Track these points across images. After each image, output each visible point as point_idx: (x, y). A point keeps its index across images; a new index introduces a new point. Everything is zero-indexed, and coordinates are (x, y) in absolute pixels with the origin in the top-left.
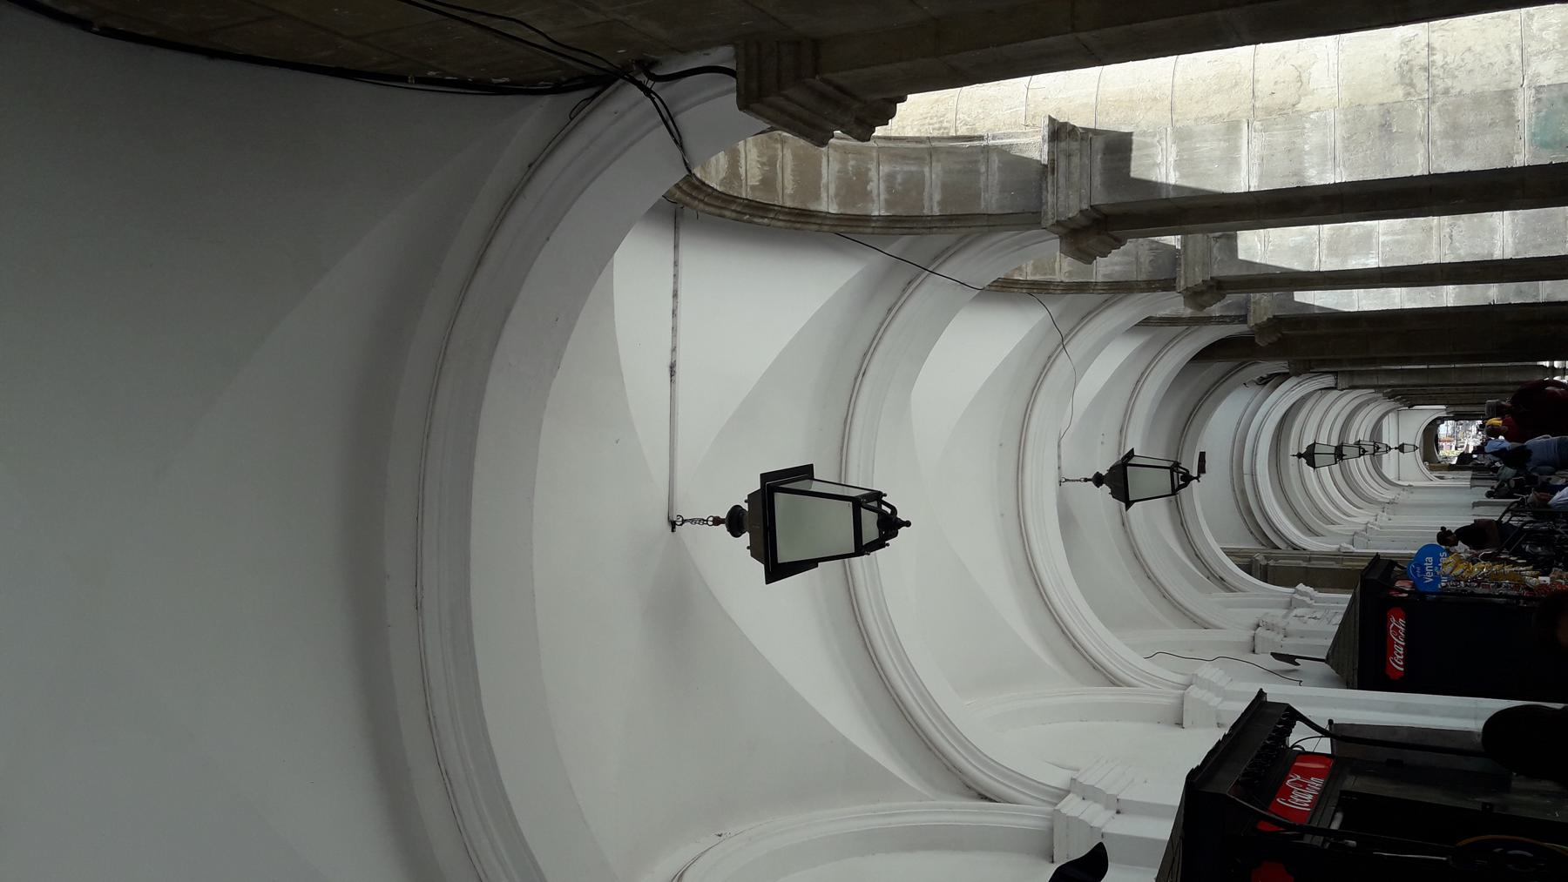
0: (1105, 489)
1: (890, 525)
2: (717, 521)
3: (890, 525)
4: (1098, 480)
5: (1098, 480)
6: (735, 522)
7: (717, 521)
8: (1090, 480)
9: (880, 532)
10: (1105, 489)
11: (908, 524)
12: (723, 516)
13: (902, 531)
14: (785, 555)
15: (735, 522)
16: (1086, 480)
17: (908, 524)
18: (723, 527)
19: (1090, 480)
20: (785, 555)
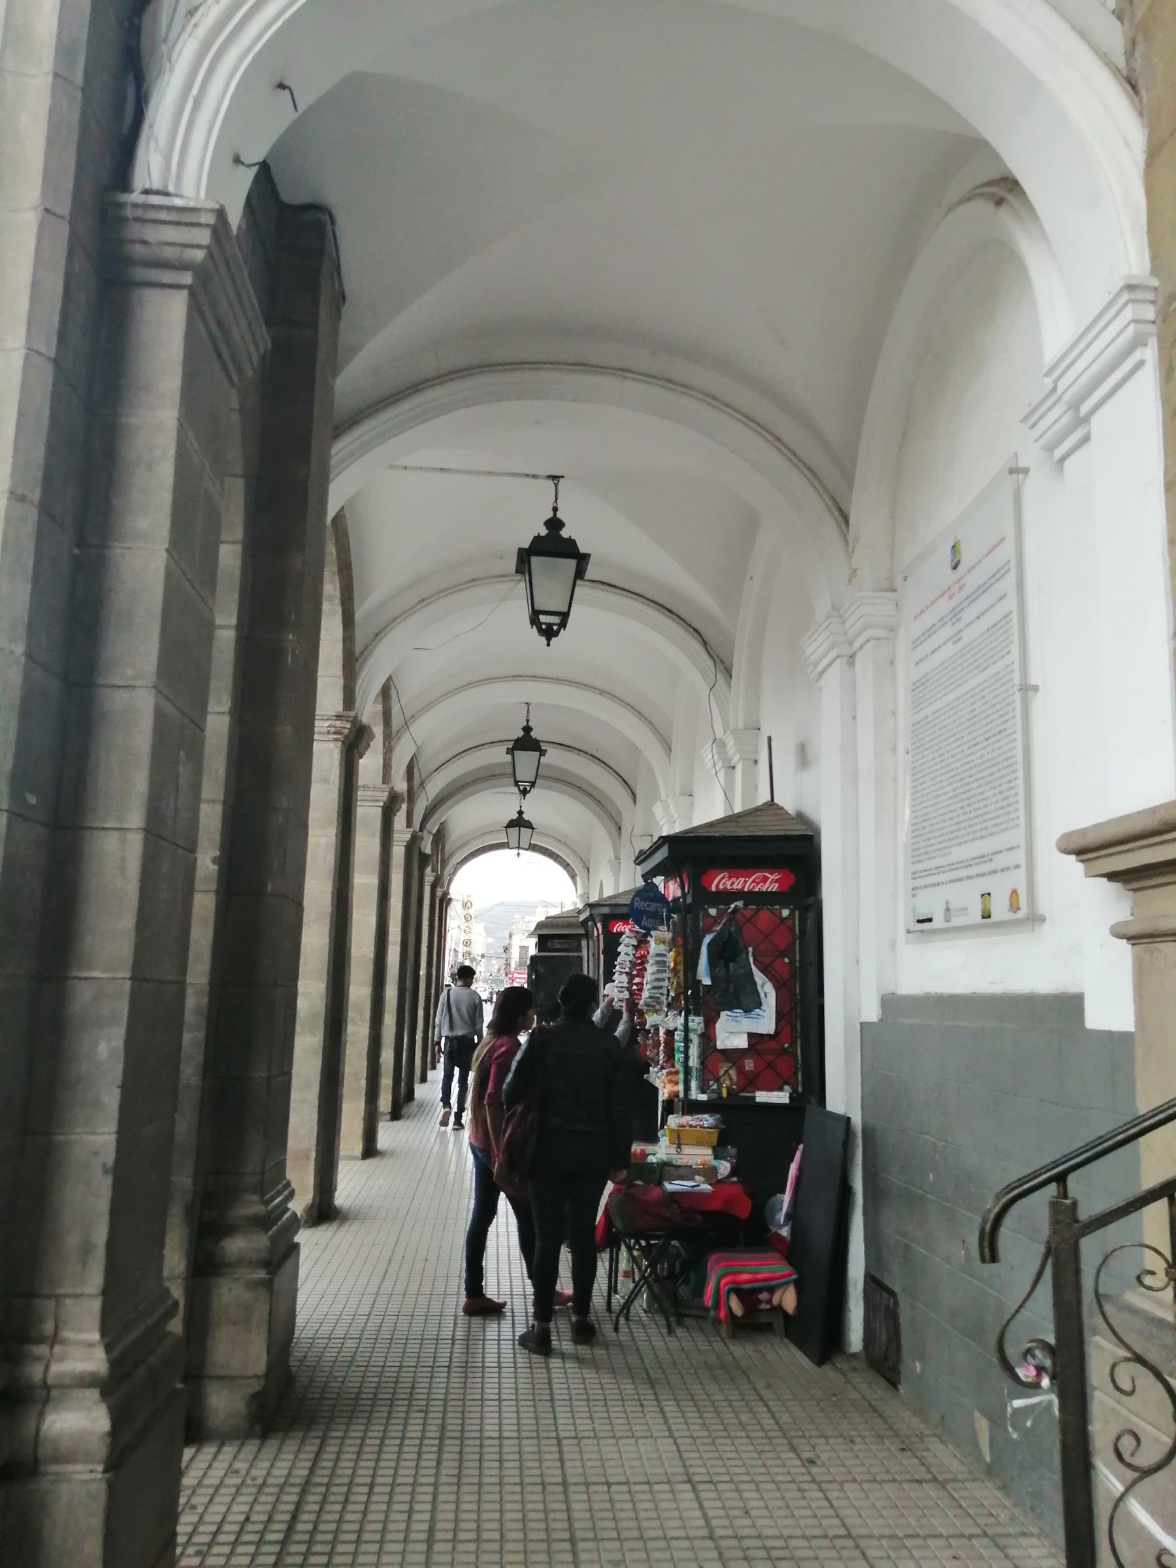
0: (521, 734)
1: (549, 633)
2: (555, 509)
3: (549, 633)
4: (527, 729)
5: (527, 729)
6: (554, 524)
7: (555, 509)
9: (544, 624)
10: (521, 734)
11: (548, 645)
12: (559, 515)
13: (543, 640)
14: (535, 560)
15: (554, 524)
16: (528, 721)
17: (548, 645)
18: (551, 515)
20: (535, 560)
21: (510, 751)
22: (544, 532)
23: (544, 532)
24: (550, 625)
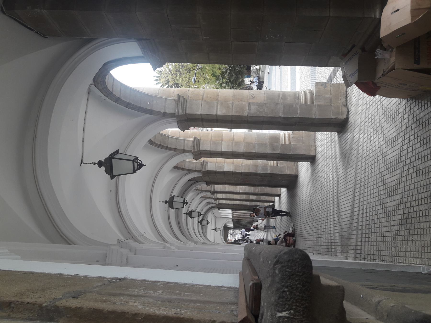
1: (141, 165)
2: (95, 164)
3: (141, 165)
4: (166, 202)
5: (166, 202)
6: (100, 164)
7: (95, 164)
8: (164, 202)
9: (138, 167)
11: (145, 165)
15: (100, 164)
16: (163, 202)
17: (145, 165)
18: (97, 165)
19: (164, 202)
21: (173, 209)
22: (103, 168)
23: (103, 168)
24: (138, 165)
